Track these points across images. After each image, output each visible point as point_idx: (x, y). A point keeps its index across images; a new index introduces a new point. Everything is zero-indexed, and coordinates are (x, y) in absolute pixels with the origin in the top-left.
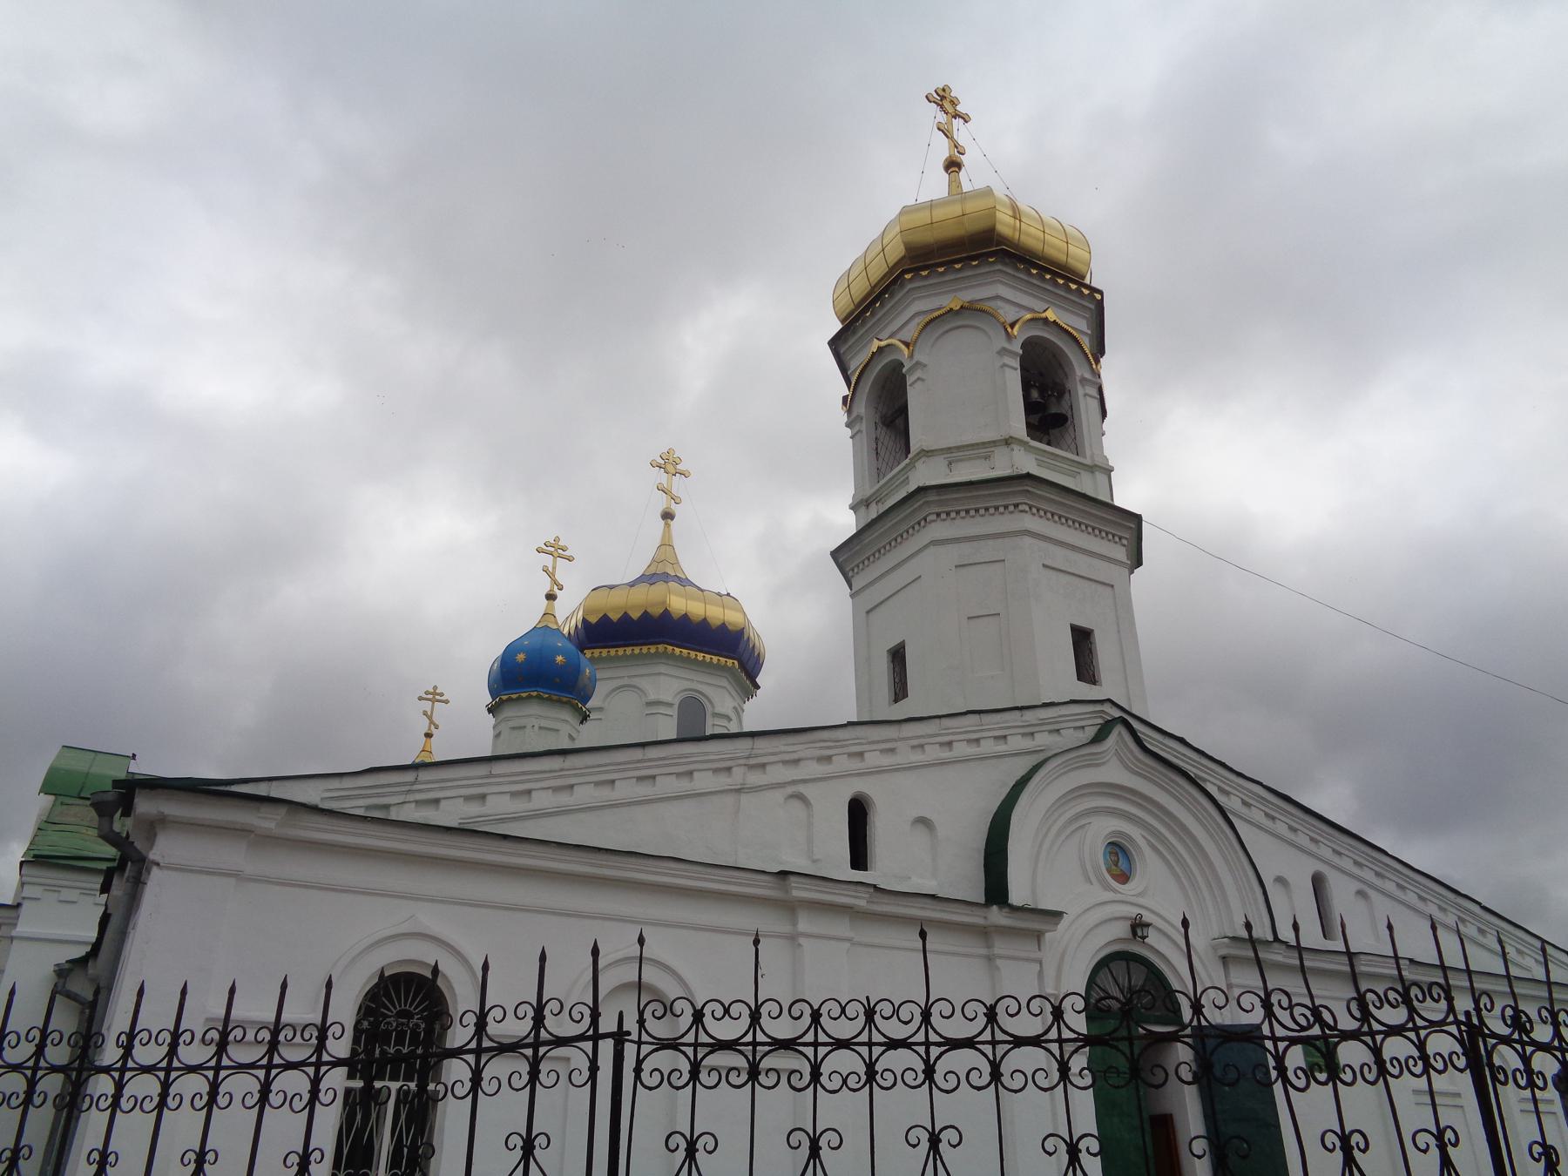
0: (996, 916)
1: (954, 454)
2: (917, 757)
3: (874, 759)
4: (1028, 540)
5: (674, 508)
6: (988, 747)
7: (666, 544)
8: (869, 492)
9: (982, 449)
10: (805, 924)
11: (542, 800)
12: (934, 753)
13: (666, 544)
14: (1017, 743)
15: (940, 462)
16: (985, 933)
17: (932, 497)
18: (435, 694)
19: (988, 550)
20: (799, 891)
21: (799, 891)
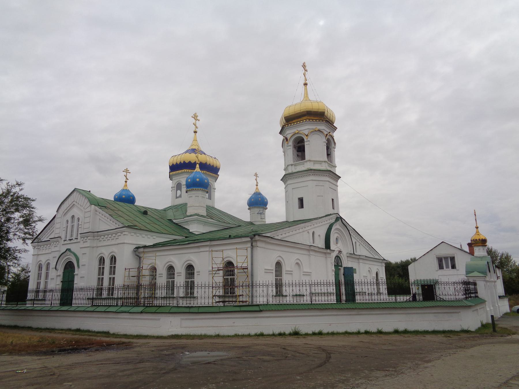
0: (328, 251)
1: (315, 162)
2: (319, 225)
3: (316, 225)
4: (328, 182)
5: (197, 130)
6: (323, 223)
7: (195, 140)
8: (293, 163)
9: (320, 162)
10: (311, 253)
11: (287, 234)
12: (321, 224)
13: (195, 140)
14: (328, 222)
15: (312, 163)
16: (325, 253)
17: (313, 171)
18: (127, 170)
19: (321, 183)
20: (312, 248)
21: (312, 248)
